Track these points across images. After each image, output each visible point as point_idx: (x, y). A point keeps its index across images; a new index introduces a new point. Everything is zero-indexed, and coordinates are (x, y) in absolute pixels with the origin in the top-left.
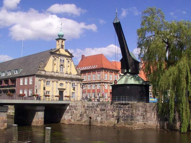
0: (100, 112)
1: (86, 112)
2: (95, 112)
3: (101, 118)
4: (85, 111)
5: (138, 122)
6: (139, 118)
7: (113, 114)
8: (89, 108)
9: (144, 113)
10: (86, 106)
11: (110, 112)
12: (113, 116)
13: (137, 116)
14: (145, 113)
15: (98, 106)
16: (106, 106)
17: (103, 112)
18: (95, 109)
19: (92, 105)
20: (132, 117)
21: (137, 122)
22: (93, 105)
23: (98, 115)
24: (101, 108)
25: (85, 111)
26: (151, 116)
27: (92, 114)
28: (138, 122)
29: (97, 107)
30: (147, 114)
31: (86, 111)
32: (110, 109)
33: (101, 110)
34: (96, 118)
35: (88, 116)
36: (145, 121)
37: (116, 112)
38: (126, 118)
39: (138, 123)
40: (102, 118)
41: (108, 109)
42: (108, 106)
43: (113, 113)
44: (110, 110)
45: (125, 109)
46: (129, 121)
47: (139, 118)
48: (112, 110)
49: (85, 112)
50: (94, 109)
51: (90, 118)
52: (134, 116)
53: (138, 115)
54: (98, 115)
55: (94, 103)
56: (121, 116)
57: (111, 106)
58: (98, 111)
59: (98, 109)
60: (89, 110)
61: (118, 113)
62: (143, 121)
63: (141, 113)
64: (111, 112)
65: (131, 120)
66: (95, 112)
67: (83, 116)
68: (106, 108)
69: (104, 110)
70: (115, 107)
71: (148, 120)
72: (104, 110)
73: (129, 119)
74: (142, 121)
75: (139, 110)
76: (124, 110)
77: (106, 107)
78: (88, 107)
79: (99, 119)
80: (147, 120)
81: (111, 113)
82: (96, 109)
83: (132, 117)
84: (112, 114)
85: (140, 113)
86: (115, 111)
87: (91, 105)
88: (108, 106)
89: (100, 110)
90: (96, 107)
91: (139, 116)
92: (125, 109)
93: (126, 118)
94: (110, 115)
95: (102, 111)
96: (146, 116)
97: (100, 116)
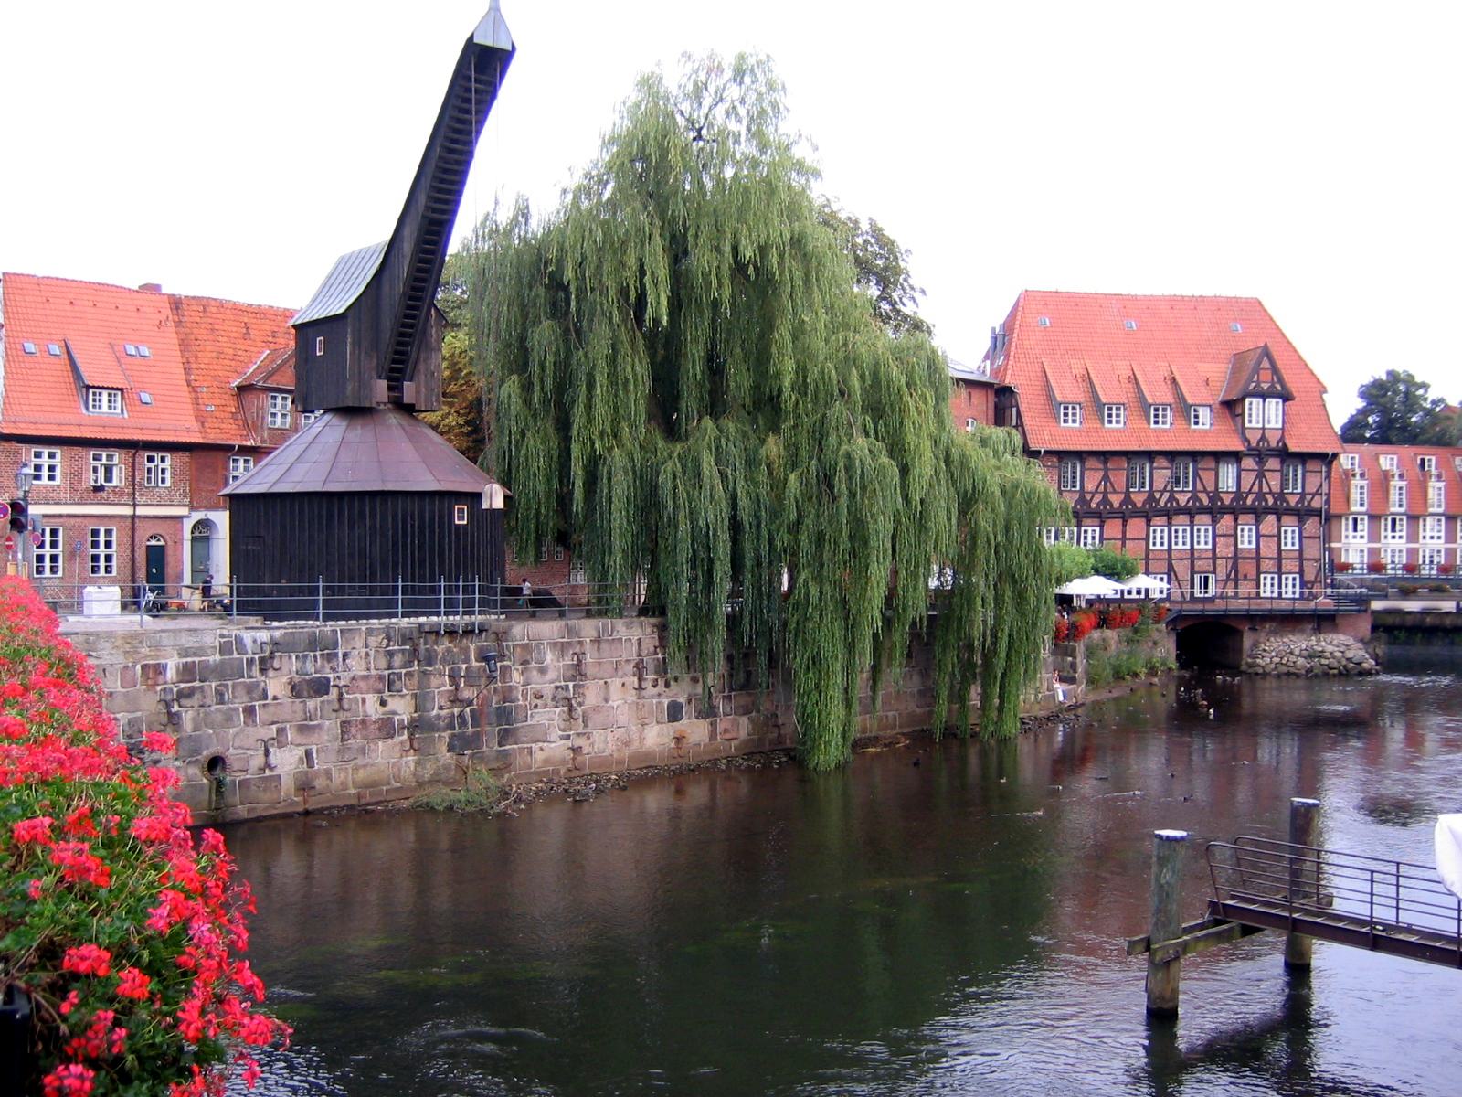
0: (292, 710)
1: (173, 719)
2: (250, 712)
3: (300, 752)
4: (169, 713)
5: (542, 749)
6: (548, 718)
7: (386, 709)
8: (197, 684)
9: (571, 684)
10: (171, 674)
11: (364, 701)
12: (387, 728)
13: (536, 706)
14: (574, 686)
15: (276, 664)
16: (336, 655)
17: (311, 704)
18: (250, 689)
19: (222, 653)
20: (505, 719)
22: (235, 655)
23: (281, 731)
24: (297, 678)
25: (169, 713)
26: (606, 700)
27: (232, 731)
28: (542, 749)
29: (263, 671)
30: (587, 693)
31: (176, 708)
32: (365, 678)
33: (296, 690)
34: (267, 753)
35: (197, 751)
36: (579, 734)
37: (405, 691)
38: (470, 730)
39: (539, 756)
40: (308, 754)
41: (348, 675)
42: (345, 656)
43: (383, 703)
44: (362, 684)
45: (464, 666)
46: (490, 746)
47: (548, 718)
49: (165, 719)
50: (241, 692)
51: (215, 763)
52: (516, 707)
53: (539, 702)
54: (281, 731)
55: (239, 640)
56: (438, 717)
57: (367, 655)
58: (275, 698)
59: (276, 685)
61: (421, 701)
62: (568, 737)
63: (557, 688)
64: (372, 699)
65: (505, 736)
66: (250, 712)
68: (333, 669)
69: (320, 687)
70: (397, 660)
71: (590, 724)
72: (320, 687)
73: (491, 731)
74: (562, 738)
75: (543, 671)
76: (454, 678)
77: (334, 664)
78: (187, 672)
79: (286, 761)
80: (586, 726)
81: (372, 708)
82: (257, 684)
83: (504, 715)
84: (381, 710)
85: (548, 690)
86: (398, 685)
87: (218, 657)
88: (345, 656)
89: (293, 689)
90: (256, 670)
91: (546, 706)
92: (464, 666)
93: (470, 730)
94: (363, 722)
95: (310, 697)
96: (580, 704)
97: (291, 734)
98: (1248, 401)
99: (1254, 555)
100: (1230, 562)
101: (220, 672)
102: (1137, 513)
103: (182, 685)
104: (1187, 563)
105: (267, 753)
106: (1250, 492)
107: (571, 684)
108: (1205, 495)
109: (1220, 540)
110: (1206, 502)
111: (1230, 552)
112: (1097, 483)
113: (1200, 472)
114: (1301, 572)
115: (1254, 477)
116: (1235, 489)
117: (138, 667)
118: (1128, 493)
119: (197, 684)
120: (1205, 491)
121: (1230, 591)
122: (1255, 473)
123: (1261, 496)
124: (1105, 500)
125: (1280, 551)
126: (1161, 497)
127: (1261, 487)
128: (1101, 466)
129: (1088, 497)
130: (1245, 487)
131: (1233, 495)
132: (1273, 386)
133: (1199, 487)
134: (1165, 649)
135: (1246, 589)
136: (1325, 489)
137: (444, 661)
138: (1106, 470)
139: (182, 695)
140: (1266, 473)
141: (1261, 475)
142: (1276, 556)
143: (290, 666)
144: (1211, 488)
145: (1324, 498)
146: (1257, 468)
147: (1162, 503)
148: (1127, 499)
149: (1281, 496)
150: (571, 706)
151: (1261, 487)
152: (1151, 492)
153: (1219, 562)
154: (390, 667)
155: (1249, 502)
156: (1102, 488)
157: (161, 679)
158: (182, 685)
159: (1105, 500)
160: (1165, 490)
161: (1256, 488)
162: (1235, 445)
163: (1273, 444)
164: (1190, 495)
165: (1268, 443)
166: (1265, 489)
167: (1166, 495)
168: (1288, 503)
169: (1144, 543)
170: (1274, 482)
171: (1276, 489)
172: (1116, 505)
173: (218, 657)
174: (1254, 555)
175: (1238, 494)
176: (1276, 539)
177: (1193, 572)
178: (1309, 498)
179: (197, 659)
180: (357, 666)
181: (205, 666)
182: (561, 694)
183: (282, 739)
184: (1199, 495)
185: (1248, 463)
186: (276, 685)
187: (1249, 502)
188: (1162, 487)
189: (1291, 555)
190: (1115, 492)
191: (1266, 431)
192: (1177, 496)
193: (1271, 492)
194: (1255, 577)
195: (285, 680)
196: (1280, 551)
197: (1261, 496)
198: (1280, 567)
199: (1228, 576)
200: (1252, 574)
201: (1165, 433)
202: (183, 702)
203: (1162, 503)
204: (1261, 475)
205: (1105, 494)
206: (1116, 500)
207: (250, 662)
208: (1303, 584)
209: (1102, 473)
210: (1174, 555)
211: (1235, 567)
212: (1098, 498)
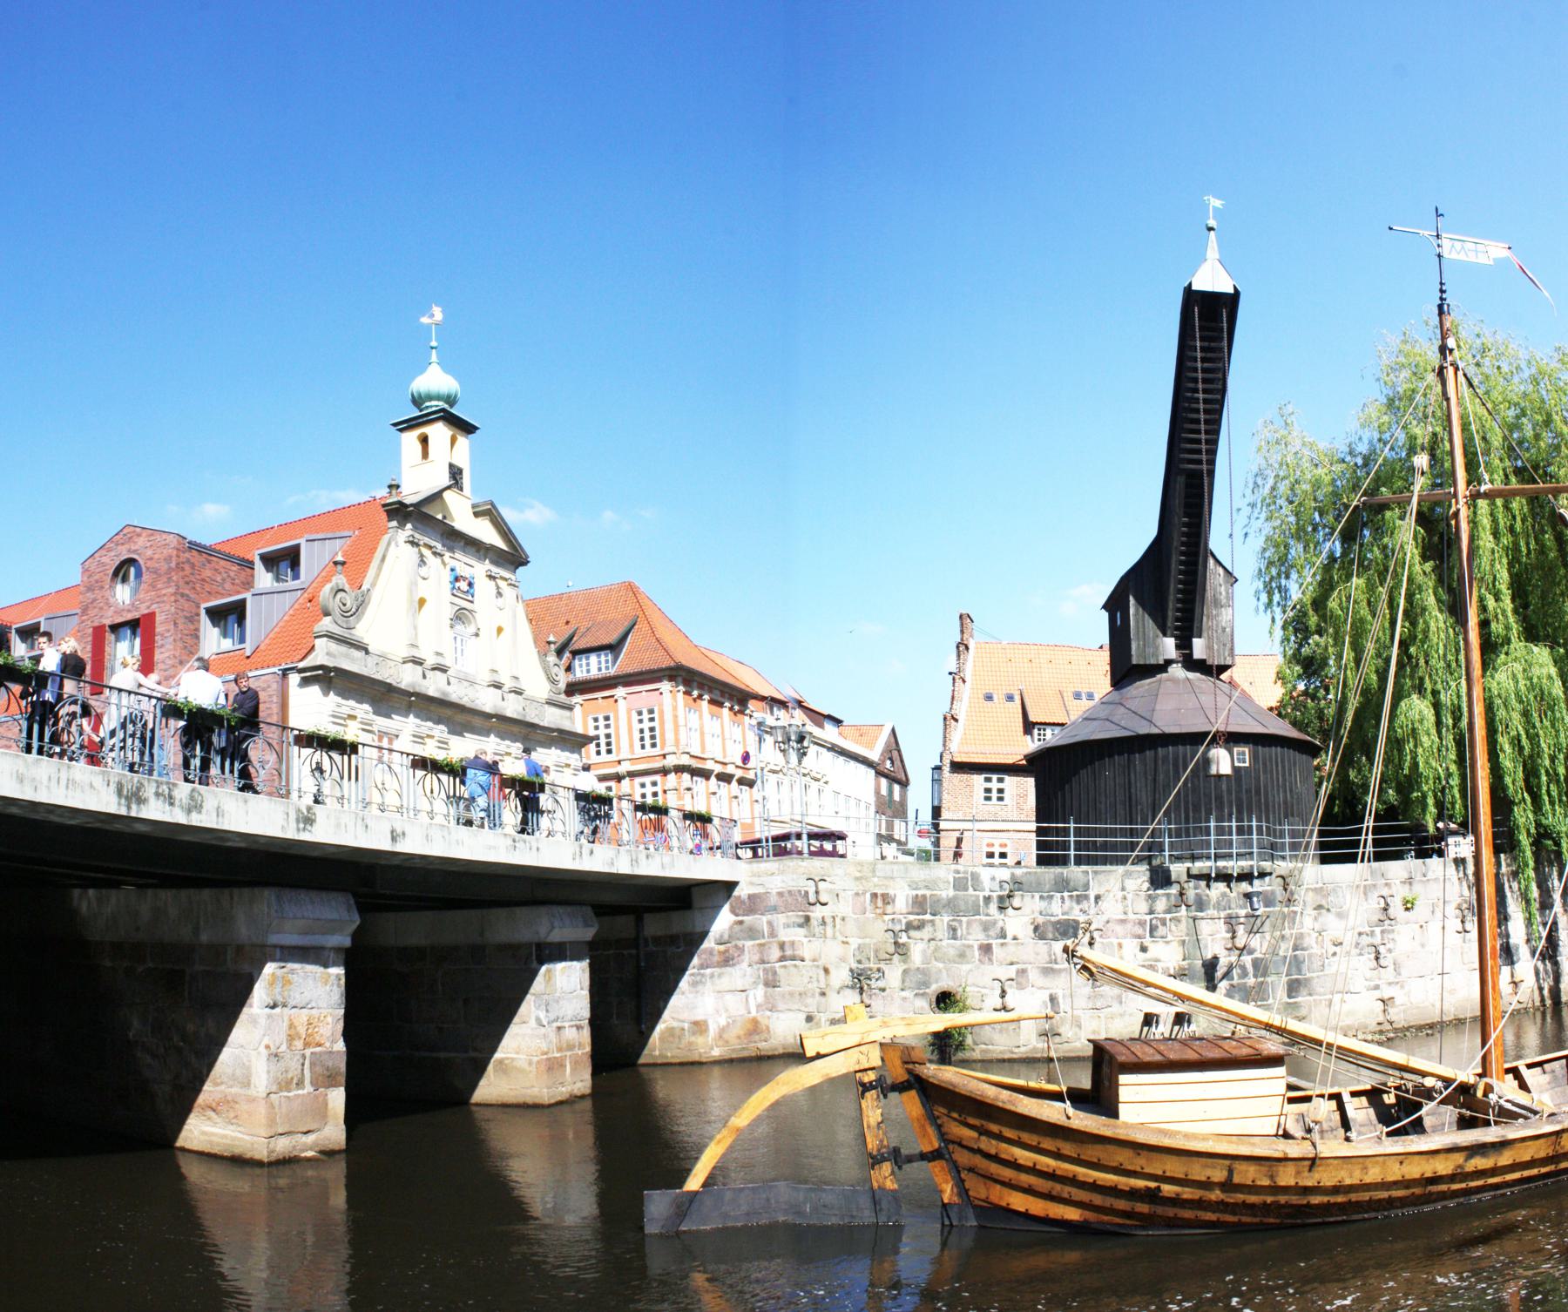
1: (901, 949)
2: (986, 949)
8: (928, 917)
9: (1378, 930)
11: (1120, 945)
14: (1382, 932)
18: (986, 928)
21: (1337, 998)
24: (1041, 920)
25: (896, 943)
29: (1002, 908)
32: (1123, 921)
33: (1039, 931)
34: (1003, 994)
36: (1390, 984)
37: (1170, 938)
40: (1053, 999)
41: (1105, 918)
42: (1098, 898)
43: (1144, 949)
44: (1119, 929)
48: (1140, 931)
49: (891, 949)
52: (1310, 956)
53: (1337, 949)
54: (1022, 972)
60: (926, 933)
62: (1377, 987)
67: (881, 984)
72: (1068, 929)
77: (1085, 905)
78: (919, 904)
79: (1028, 1002)
85: (1349, 939)
86: (1161, 930)
87: (951, 893)
88: (1098, 898)
89: (1036, 929)
90: (993, 907)
95: (1055, 939)
96: (1390, 951)
97: (1034, 975)
101: (952, 906)
103: (912, 917)
105: (1003, 994)
107: (1378, 930)
117: (868, 896)
119: (928, 917)
137: (1218, 906)
139: (910, 927)
143: (1030, 907)
150: (1378, 952)
154: (1151, 912)
157: (889, 909)
158: (912, 917)
173: (951, 893)
179: (928, 893)
180: (1111, 908)
181: (937, 900)
182: (1365, 940)
183: (1023, 981)
186: (1017, 923)
195: (1028, 919)
202: (912, 933)
207: (988, 899)
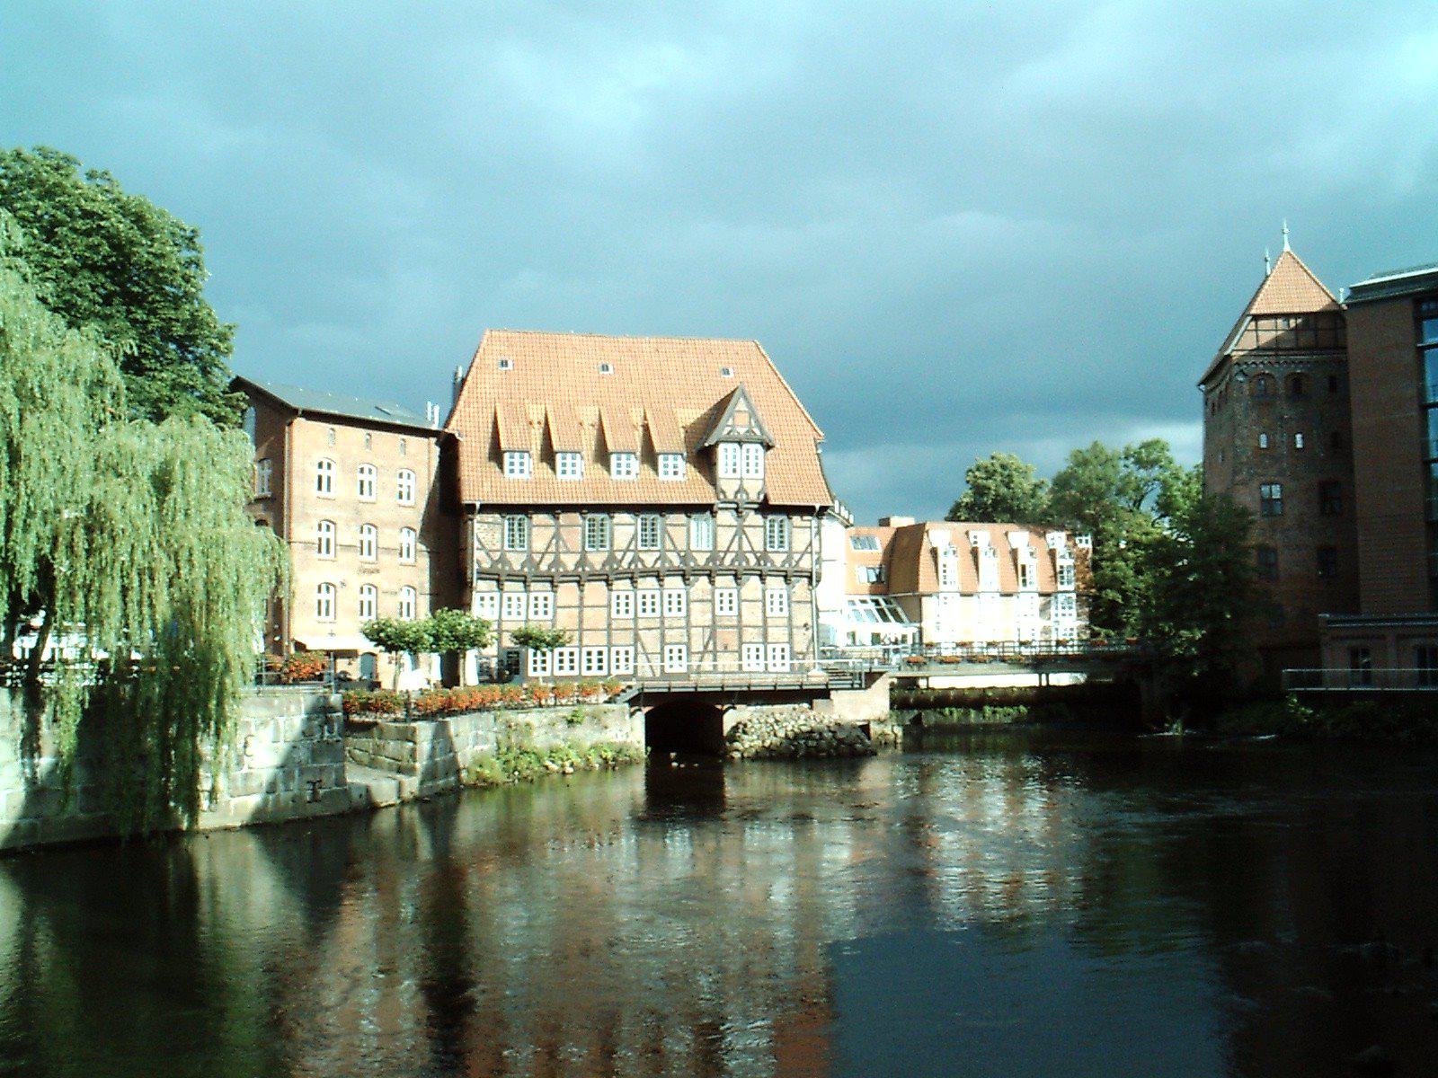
98: (721, 447)
99: (735, 623)
100: (708, 631)
102: (595, 576)
104: (657, 633)
106: (727, 551)
108: (675, 554)
109: (695, 607)
110: (676, 562)
111: (707, 620)
112: (547, 541)
113: (669, 528)
114: (790, 642)
115: (732, 534)
116: (711, 548)
118: (584, 552)
120: (675, 550)
121: (707, 664)
122: (735, 529)
123: (740, 555)
124: (557, 562)
125: (765, 619)
126: (623, 558)
127: (740, 546)
128: (552, 522)
129: (537, 558)
130: (723, 545)
131: (709, 554)
132: (750, 431)
133: (669, 545)
134: (630, 732)
135: (727, 661)
136: (816, 547)
138: (558, 527)
140: (746, 529)
141: (741, 531)
142: (761, 624)
144: (682, 546)
145: (815, 557)
146: (735, 523)
147: (625, 565)
148: (582, 562)
149: (763, 556)
151: (740, 546)
152: (612, 552)
153: (693, 631)
155: (727, 562)
156: (553, 548)
159: (557, 562)
160: (628, 550)
161: (735, 547)
162: (704, 494)
163: (753, 497)
164: (657, 554)
165: (747, 494)
166: (746, 547)
167: (630, 556)
168: (773, 563)
169: (605, 611)
170: (756, 538)
171: (759, 547)
172: (571, 567)
174: (735, 623)
175: (714, 555)
176: (760, 604)
177: (663, 643)
178: (796, 557)
184: (669, 554)
185: (726, 517)
187: (727, 562)
188: (624, 546)
189: (778, 622)
190: (568, 552)
191: (745, 482)
192: (642, 556)
193: (753, 551)
194: (736, 648)
196: (765, 619)
197: (740, 555)
198: (765, 636)
199: (706, 647)
200: (734, 645)
201: (627, 478)
203: (625, 565)
204: (741, 531)
205: (557, 553)
206: (570, 562)
208: (793, 655)
209: (552, 531)
210: (642, 624)
211: (713, 636)
212: (549, 559)
